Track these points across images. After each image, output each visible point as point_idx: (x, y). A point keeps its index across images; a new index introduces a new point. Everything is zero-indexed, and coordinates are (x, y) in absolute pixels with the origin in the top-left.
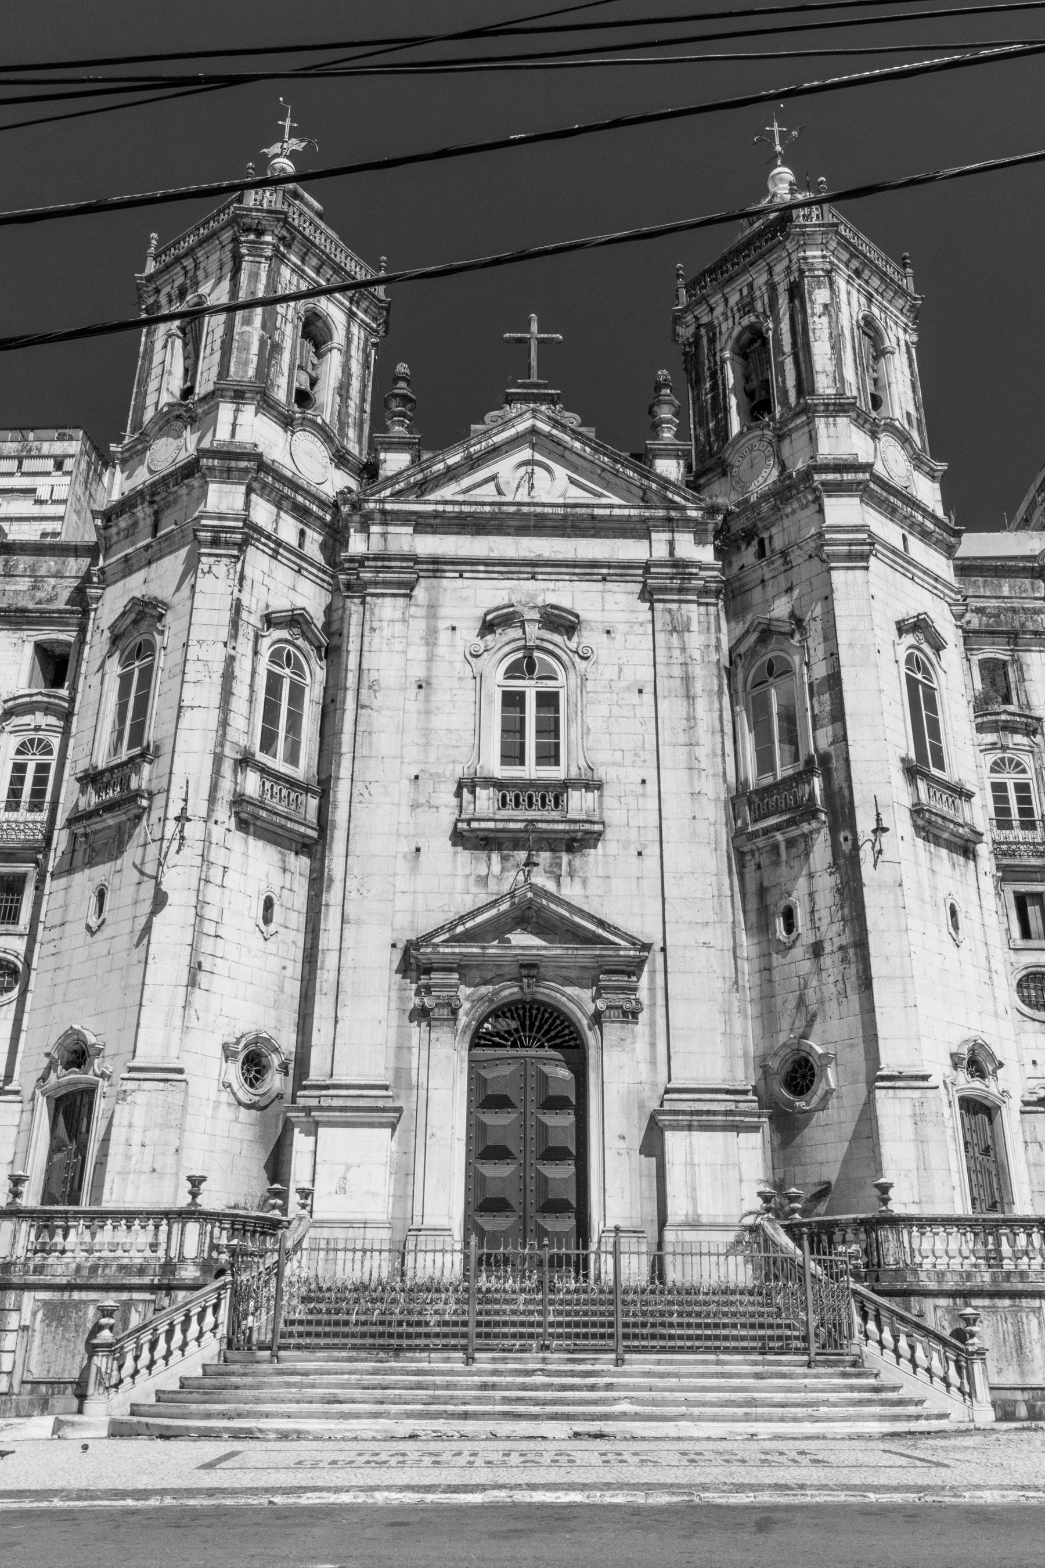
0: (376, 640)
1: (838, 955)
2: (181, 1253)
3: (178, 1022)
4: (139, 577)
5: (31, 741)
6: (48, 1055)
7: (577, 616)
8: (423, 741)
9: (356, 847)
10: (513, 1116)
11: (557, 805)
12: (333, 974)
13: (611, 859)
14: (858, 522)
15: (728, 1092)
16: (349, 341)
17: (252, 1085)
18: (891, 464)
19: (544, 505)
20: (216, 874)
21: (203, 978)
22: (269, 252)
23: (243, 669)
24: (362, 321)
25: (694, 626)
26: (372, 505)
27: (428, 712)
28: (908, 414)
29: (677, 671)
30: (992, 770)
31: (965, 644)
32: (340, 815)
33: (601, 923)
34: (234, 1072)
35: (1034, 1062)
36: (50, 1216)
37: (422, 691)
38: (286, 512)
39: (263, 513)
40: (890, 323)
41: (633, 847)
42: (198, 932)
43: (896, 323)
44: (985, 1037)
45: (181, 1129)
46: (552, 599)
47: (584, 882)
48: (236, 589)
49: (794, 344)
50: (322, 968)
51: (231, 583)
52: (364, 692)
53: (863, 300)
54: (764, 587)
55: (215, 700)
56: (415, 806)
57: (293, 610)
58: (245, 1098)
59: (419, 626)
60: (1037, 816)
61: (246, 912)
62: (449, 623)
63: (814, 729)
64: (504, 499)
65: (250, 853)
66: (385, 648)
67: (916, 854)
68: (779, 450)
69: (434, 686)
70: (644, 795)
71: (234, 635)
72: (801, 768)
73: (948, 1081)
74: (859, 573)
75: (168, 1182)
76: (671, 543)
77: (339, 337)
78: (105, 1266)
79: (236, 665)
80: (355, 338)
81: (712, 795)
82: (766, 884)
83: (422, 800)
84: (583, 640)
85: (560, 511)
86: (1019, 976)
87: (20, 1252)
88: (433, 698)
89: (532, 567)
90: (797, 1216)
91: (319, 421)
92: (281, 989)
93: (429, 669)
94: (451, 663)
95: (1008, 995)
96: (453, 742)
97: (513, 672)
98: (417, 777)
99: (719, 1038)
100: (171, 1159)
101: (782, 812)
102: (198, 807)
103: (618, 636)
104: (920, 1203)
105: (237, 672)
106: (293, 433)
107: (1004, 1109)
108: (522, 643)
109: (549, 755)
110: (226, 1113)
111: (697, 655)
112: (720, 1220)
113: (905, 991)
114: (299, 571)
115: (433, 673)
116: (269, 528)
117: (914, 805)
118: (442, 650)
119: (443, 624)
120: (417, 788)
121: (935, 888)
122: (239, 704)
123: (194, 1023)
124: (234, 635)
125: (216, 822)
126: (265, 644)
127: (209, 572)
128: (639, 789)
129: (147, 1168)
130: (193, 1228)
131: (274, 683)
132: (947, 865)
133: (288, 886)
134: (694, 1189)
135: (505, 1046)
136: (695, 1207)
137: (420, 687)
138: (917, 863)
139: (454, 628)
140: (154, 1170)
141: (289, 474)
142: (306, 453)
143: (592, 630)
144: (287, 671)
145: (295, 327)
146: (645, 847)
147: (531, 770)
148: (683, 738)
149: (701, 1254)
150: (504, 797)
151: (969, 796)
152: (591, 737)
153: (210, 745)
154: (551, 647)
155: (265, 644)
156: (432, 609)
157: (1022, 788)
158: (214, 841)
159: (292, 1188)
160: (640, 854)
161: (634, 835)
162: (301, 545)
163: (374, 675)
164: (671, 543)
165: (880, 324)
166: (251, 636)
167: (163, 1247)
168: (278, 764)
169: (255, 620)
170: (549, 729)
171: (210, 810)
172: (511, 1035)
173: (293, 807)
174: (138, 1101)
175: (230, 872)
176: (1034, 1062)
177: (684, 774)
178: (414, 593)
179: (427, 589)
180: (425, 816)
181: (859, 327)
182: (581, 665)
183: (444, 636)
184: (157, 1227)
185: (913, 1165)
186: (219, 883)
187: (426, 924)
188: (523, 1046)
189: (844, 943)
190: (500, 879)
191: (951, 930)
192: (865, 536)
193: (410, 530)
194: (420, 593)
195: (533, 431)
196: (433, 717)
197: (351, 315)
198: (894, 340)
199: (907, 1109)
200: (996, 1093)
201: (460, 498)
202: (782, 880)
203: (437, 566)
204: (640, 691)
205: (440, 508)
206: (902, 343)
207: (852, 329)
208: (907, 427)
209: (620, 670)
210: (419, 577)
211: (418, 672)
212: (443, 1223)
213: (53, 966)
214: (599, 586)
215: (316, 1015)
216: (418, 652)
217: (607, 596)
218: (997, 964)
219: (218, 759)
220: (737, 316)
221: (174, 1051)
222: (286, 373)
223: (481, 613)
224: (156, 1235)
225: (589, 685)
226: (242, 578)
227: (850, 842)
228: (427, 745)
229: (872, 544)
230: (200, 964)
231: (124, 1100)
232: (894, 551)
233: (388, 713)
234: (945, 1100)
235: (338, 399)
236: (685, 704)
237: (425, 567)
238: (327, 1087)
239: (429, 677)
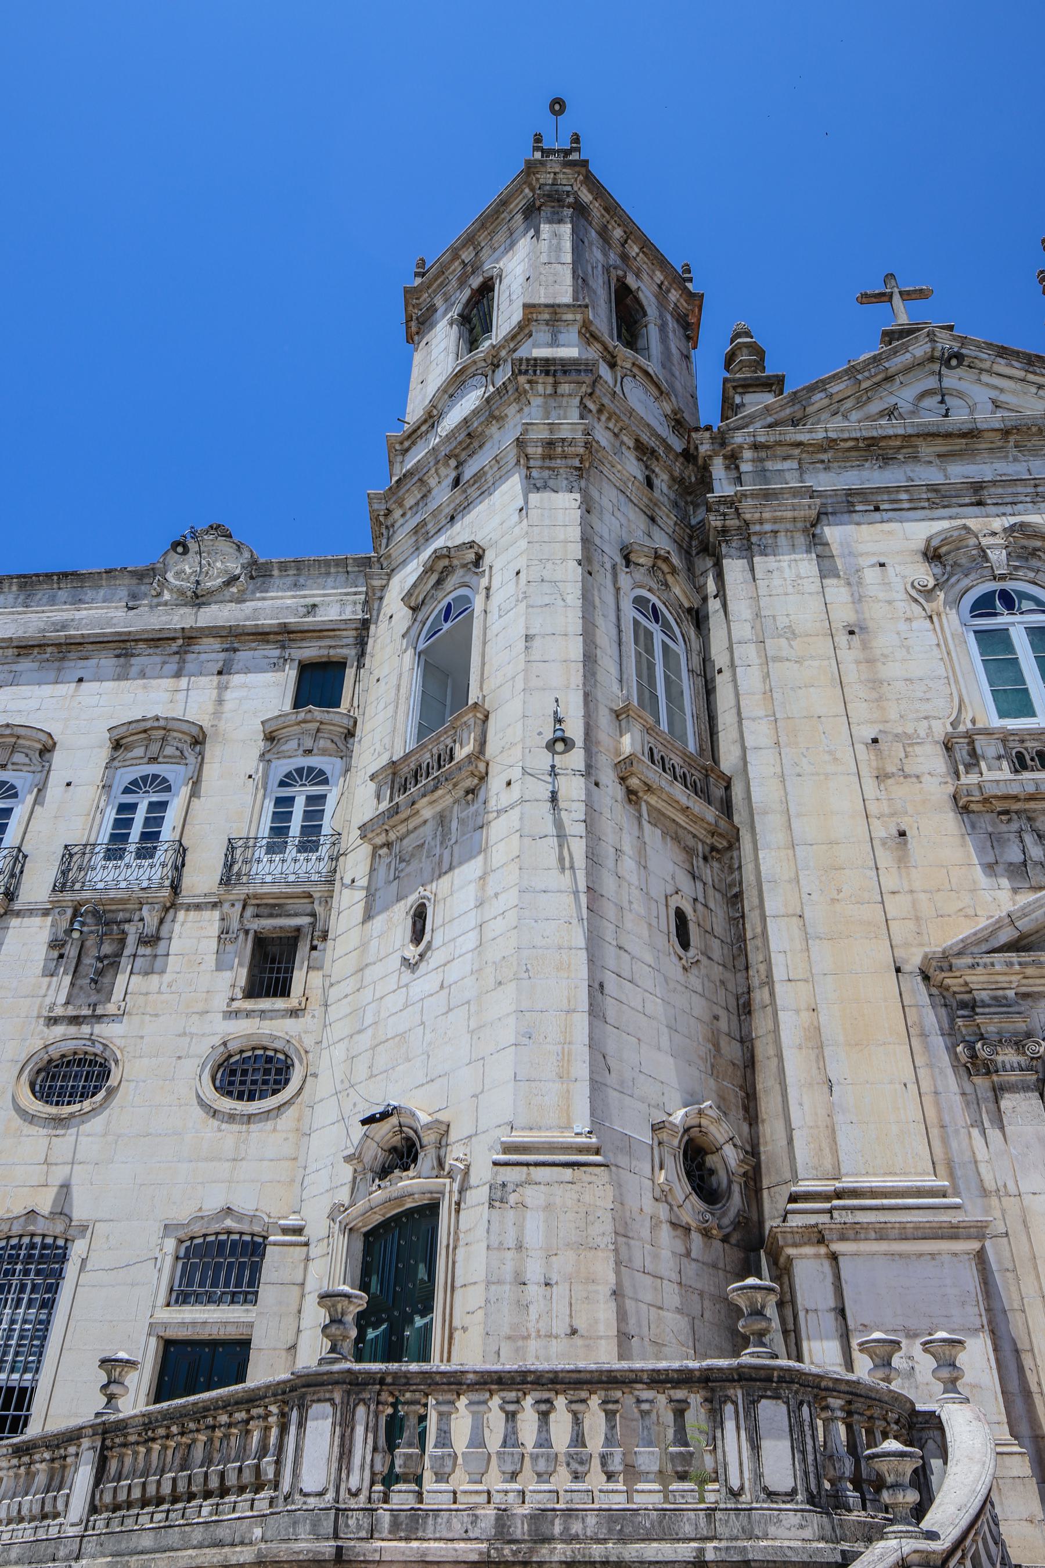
27: (871, 661)
37: (855, 638)
62: (874, 560)
65: (647, 839)
92: (717, 1046)
98: (875, 741)
120: (879, 754)
196: (879, 664)
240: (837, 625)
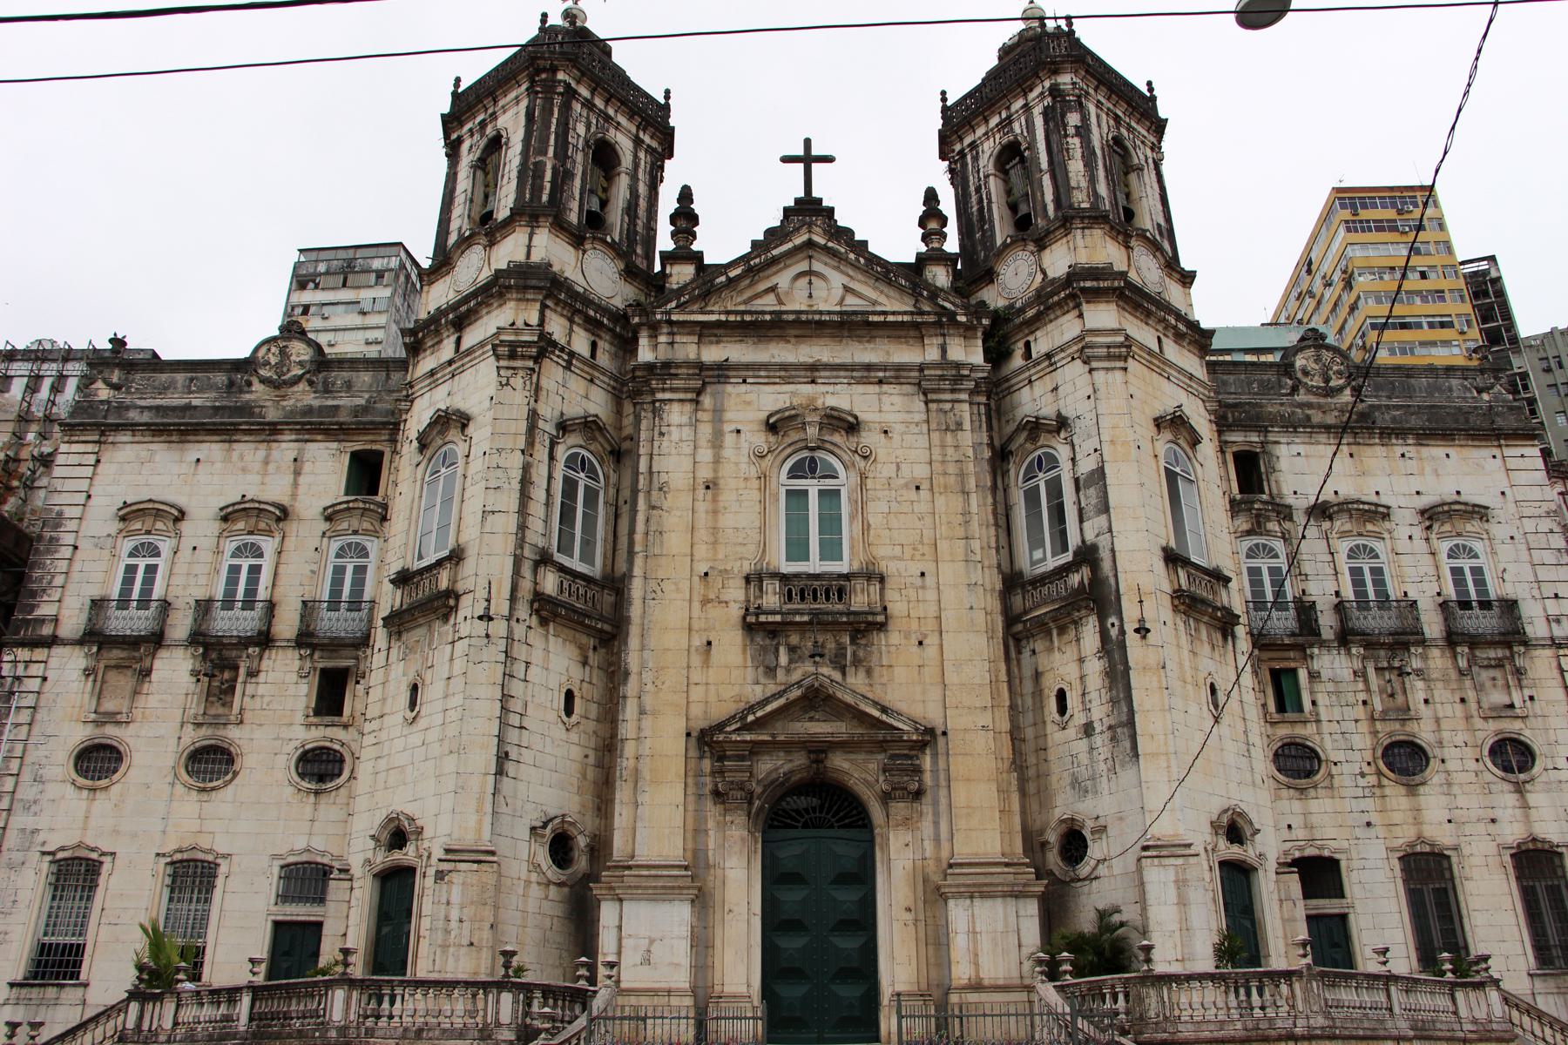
0: (665, 444)
1: (1108, 735)
2: (497, 1020)
3: (489, 809)
4: (442, 391)
5: (349, 545)
6: (373, 837)
7: (856, 417)
8: (712, 539)
9: (652, 642)
10: (806, 892)
11: (840, 599)
12: (632, 762)
13: (893, 649)
14: (1115, 325)
15: (1007, 865)
16: (636, 165)
17: (560, 866)
18: (1145, 272)
19: (821, 313)
20: (519, 669)
21: (510, 768)
22: (561, 89)
23: (540, 473)
24: (649, 146)
25: (967, 425)
26: (659, 317)
27: (715, 512)
28: (1159, 225)
29: (952, 468)
30: (1248, 556)
31: (1219, 436)
32: (635, 611)
33: (884, 710)
34: (543, 857)
35: (1289, 826)
36: (379, 985)
38: (579, 325)
39: (557, 327)
40: (1138, 143)
41: (913, 636)
42: (503, 723)
43: (1143, 142)
44: (1243, 806)
45: (496, 907)
46: (831, 401)
47: (869, 672)
48: (532, 400)
49: (1051, 162)
50: (621, 757)
51: (528, 394)
52: (654, 493)
53: (1112, 122)
54: (1031, 387)
55: (514, 505)
56: (705, 602)
57: (586, 417)
58: (554, 878)
59: (706, 430)
60: (1290, 598)
61: (549, 705)
62: (733, 427)
63: (1081, 521)
64: (784, 308)
66: (674, 451)
67: (1177, 637)
68: (1040, 259)
69: (721, 486)
70: (923, 587)
71: (530, 442)
72: (1070, 558)
73: (1209, 848)
74: (1119, 375)
75: (486, 955)
76: (944, 351)
77: (626, 161)
78: (429, 1030)
79: (533, 471)
80: (643, 163)
81: (988, 587)
82: (1040, 669)
83: (712, 596)
84: (862, 440)
85: (836, 318)
86: (1275, 748)
87: (352, 1017)
88: (720, 498)
89: (812, 371)
90: (1068, 977)
91: (609, 239)
93: (715, 471)
94: (737, 464)
95: (1263, 764)
96: (740, 540)
97: (795, 473)
98: (706, 574)
99: (997, 814)
100: (486, 934)
101: (1053, 601)
102: (501, 606)
103: (895, 436)
104: (1183, 960)
105: (535, 478)
106: (584, 252)
107: (1261, 873)
108: (802, 444)
109: (831, 549)
110: (536, 891)
111: (970, 452)
112: (1001, 982)
113: (1168, 767)
114: (591, 381)
115: (720, 475)
116: (563, 341)
117: (1175, 592)
118: (728, 453)
119: (728, 427)
120: (707, 586)
121: (1197, 669)
122: (537, 508)
123: (503, 809)
124: (530, 442)
125: (518, 620)
126: (562, 453)
127: (507, 384)
128: (919, 581)
129: (465, 942)
130: (506, 997)
131: (570, 486)
132: (1207, 648)
133: (587, 679)
134: (976, 955)
135: (797, 827)
136: (977, 971)
137: (708, 488)
138: (1178, 646)
139: (738, 431)
140: (472, 944)
141: (581, 290)
142: (597, 270)
143: (870, 430)
144: (582, 475)
145: (586, 155)
146: (926, 636)
147: (814, 564)
148: (961, 532)
149: (985, 1015)
150: (790, 591)
151: (1227, 580)
152: (872, 532)
153: (511, 548)
154: (831, 448)
155: (562, 453)
156: (718, 413)
157: (1274, 571)
158: (516, 638)
159: (600, 958)
160: (920, 643)
161: (914, 625)
162: (593, 355)
163: (664, 477)
164: (944, 351)
165: (1128, 144)
166: (547, 443)
167: (481, 1013)
168: (575, 564)
169: (550, 428)
170: (831, 523)
171: (512, 609)
172: (803, 817)
173: (590, 604)
174: (455, 881)
175: (532, 667)
176: (1289, 826)
177: (961, 566)
178: (701, 398)
179: (713, 395)
180: (715, 612)
181: (1109, 146)
182: (861, 463)
183: (729, 439)
184: (474, 996)
185: (1176, 927)
186: (522, 677)
187: (719, 712)
188: (814, 827)
189: (1113, 723)
190: (788, 670)
191: (1212, 707)
192: (1121, 339)
193: (695, 339)
194: (707, 400)
195: (810, 244)
196: (720, 515)
197: (638, 142)
198: (1142, 157)
199: (1171, 875)
200: (1253, 855)
201: (742, 308)
202: (1055, 665)
203: (722, 372)
204: (918, 488)
205: (723, 318)
206: (1150, 161)
207: (1103, 149)
208: (1158, 238)
209: (898, 468)
210: (704, 384)
211: (705, 473)
212: (743, 989)
213: (375, 755)
214: (876, 388)
215: (617, 801)
216: (705, 455)
217: (884, 398)
218: (1255, 738)
219: (518, 561)
220: (997, 136)
221: (486, 835)
222: (577, 198)
223: (763, 415)
224: (474, 1003)
225: (869, 481)
226: (538, 389)
227: (1116, 628)
228: (715, 543)
229: (1129, 347)
230: (507, 754)
231: (442, 879)
232: (1150, 352)
233: (678, 513)
234: (1206, 867)
235: (626, 219)
236: (961, 499)
237: (711, 373)
238: (629, 868)
239: (717, 478)
240: (700, 481)
